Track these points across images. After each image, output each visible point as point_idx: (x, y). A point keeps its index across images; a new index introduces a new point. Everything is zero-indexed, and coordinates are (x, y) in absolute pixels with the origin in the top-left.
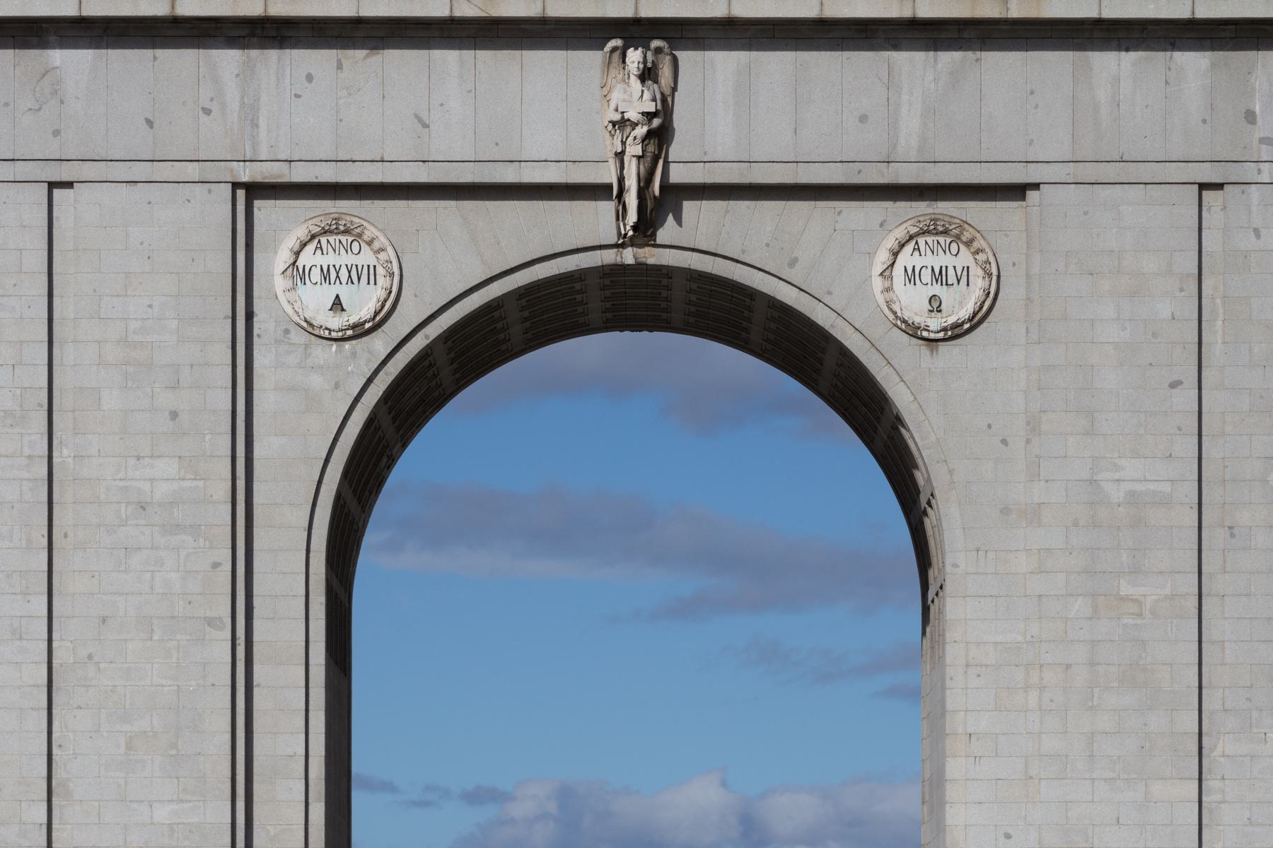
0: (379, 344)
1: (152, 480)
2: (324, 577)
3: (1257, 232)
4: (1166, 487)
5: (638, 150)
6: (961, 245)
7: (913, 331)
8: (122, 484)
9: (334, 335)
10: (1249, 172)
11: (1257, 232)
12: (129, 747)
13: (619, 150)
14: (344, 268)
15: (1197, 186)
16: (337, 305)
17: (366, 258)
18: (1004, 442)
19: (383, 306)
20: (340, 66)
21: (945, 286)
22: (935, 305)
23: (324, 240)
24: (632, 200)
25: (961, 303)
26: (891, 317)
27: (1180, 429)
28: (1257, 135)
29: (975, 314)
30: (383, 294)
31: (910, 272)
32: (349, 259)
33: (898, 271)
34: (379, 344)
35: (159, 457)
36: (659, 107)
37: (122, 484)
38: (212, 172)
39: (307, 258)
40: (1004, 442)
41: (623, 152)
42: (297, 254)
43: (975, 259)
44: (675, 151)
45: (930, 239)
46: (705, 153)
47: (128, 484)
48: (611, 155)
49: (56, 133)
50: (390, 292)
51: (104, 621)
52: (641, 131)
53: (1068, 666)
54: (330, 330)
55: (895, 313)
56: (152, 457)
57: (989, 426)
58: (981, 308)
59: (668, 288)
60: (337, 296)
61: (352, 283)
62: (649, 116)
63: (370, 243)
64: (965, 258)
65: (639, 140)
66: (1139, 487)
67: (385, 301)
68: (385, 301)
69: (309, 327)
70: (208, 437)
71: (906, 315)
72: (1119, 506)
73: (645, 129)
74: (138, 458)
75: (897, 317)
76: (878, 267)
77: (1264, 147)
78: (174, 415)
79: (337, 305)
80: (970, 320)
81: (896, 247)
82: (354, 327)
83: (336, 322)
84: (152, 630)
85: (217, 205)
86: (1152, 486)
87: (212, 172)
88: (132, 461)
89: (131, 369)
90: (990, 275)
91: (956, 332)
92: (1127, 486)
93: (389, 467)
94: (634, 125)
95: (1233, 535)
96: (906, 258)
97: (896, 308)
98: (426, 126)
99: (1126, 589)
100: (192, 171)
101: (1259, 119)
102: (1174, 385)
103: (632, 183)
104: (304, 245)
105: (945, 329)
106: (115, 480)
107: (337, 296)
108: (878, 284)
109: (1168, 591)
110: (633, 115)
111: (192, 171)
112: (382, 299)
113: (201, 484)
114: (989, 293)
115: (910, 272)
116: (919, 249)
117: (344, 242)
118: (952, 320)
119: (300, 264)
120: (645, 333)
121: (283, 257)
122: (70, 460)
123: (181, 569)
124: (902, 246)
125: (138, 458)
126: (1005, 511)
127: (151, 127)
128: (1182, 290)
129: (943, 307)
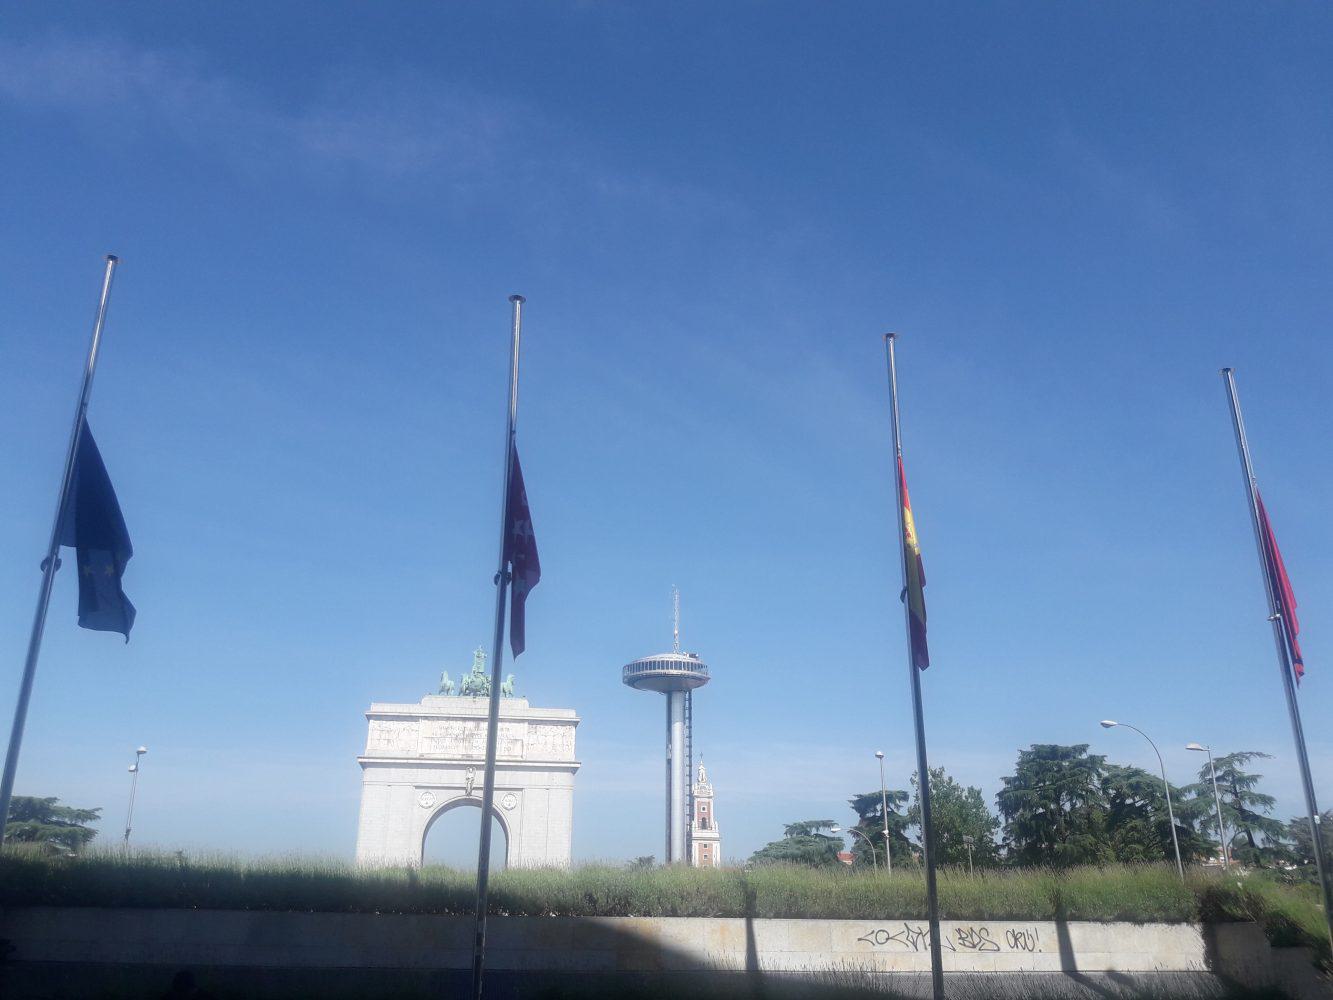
7: (506, 808)
24: (469, 790)
34: (432, 809)
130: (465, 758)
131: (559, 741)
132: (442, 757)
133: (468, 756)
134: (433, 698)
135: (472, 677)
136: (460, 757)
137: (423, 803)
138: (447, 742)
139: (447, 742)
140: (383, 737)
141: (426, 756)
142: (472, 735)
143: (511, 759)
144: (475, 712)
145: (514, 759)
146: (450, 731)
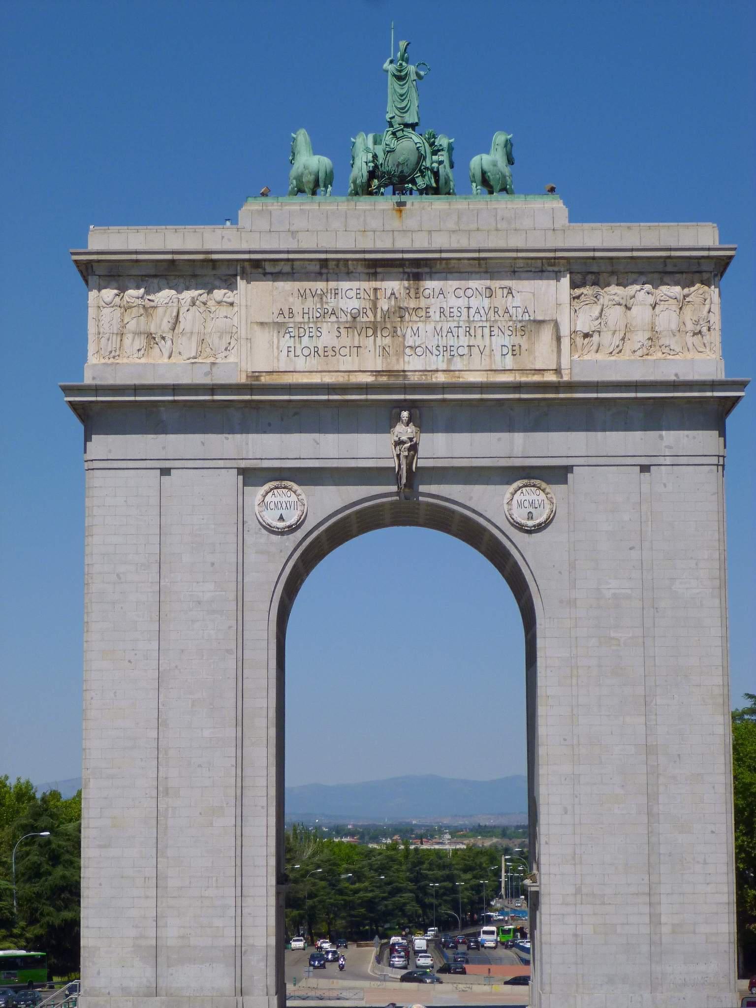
0: (299, 534)
1: (203, 592)
2: (276, 631)
3: (665, 485)
4: (629, 591)
5: (406, 453)
6: (541, 491)
7: (520, 528)
8: (191, 593)
9: (279, 530)
10: (661, 460)
11: (665, 485)
12: (193, 705)
13: (398, 453)
14: (284, 502)
15: (639, 467)
16: (281, 518)
17: (294, 498)
18: (560, 573)
19: (300, 518)
20: (282, 420)
21: (534, 509)
22: (530, 516)
23: (275, 491)
25: (541, 515)
26: (512, 521)
27: (634, 567)
28: (664, 445)
29: (547, 519)
30: (301, 514)
31: (519, 502)
32: (287, 499)
33: (514, 502)
34: (299, 534)
35: (206, 582)
36: (415, 435)
37: (191, 593)
38: (229, 464)
39: (268, 498)
40: (560, 573)
41: (400, 454)
42: (265, 496)
43: (547, 497)
44: (421, 453)
45: (527, 488)
46: (434, 454)
47: (193, 593)
48: (395, 455)
49: (164, 448)
50: (303, 513)
51: (182, 652)
52: (408, 445)
53: (589, 667)
54: (278, 529)
55: (513, 519)
56: (203, 582)
57: (554, 566)
58: (549, 517)
59: (418, 509)
60: (281, 514)
61: (288, 509)
62: (411, 439)
63: (295, 492)
64: (543, 496)
65: (406, 450)
66: (617, 591)
67: (301, 516)
68: (301, 516)
69: (270, 530)
70: (227, 574)
71: (519, 520)
72: (609, 599)
73: (409, 444)
74: (198, 582)
75: (515, 521)
76: (506, 501)
77: (667, 449)
78: (213, 564)
79: (281, 518)
80: (545, 522)
81: (513, 492)
82: (289, 527)
83: (281, 525)
84: (203, 655)
85: (232, 479)
86: (623, 591)
87: (229, 464)
88: (195, 584)
89: (194, 545)
90: (553, 503)
91: (540, 528)
92: (613, 591)
93: (301, 584)
94: (403, 443)
95: (657, 612)
96: (517, 496)
97: (513, 517)
98: (318, 444)
99: (613, 635)
100: (221, 464)
101: (665, 439)
102: (631, 549)
103: (404, 467)
104: (267, 493)
105: (534, 526)
106: (187, 592)
107: (281, 514)
108: (506, 507)
109: (630, 635)
110: (404, 438)
111: (221, 464)
112: (300, 515)
113: (224, 593)
114: (552, 511)
115: (519, 502)
116: (523, 493)
117: (284, 492)
118: (537, 522)
119: (266, 501)
120: (408, 527)
121: (259, 497)
122: (169, 584)
123: (216, 629)
124: (516, 492)
125: (198, 582)
126: (561, 602)
127: (204, 445)
128: (634, 509)
129: (534, 516)
130: (384, 379)
131: (667, 318)
132: (316, 379)
133: (389, 373)
134: (272, 205)
135: (388, 138)
136: (368, 379)
137: (271, 518)
138: (327, 337)
139: (327, 337)
140: (132, 325)
141: (265, 379)
142: (400, 312)
143: (524, 379)
144: (403, 243)
145: (536, 378)
146: (331, 303)
